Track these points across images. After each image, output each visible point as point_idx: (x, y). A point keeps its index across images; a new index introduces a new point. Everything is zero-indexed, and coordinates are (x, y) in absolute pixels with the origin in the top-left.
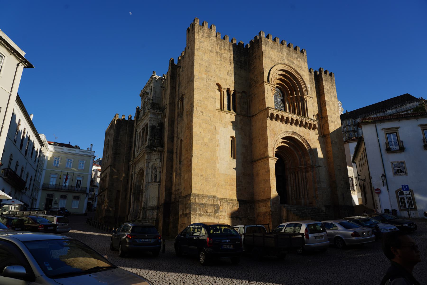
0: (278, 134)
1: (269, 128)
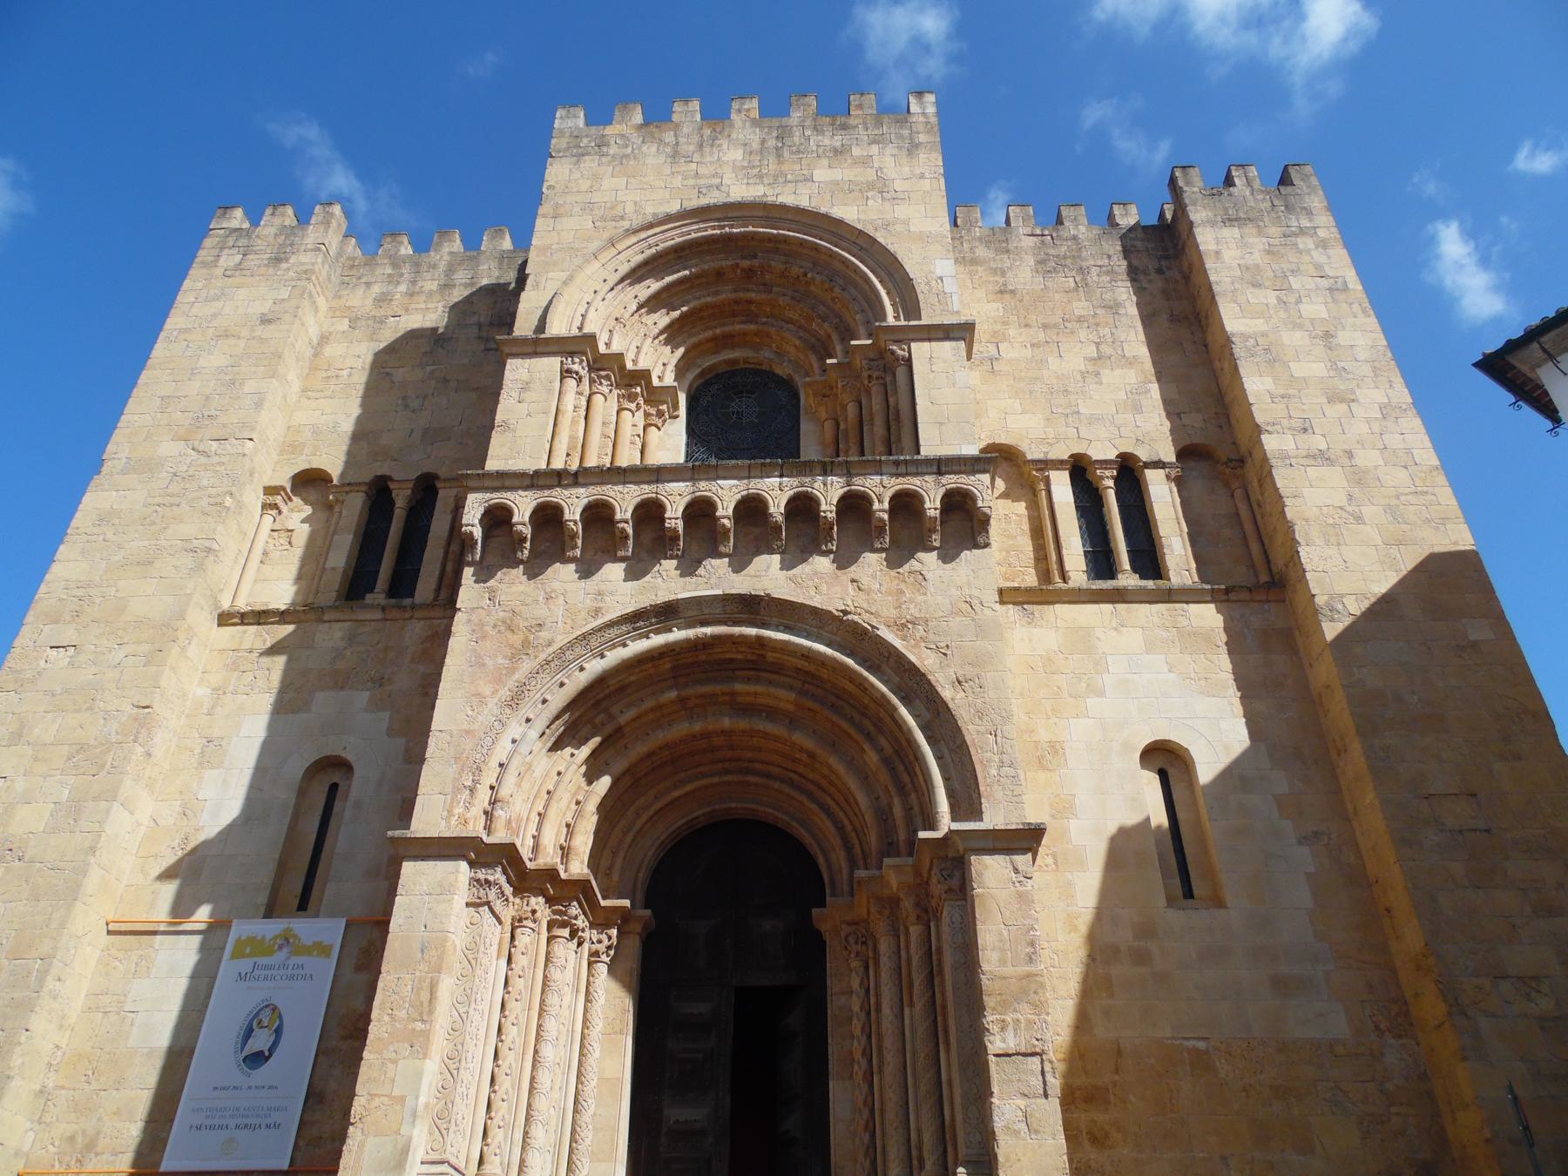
1: (469, 621)
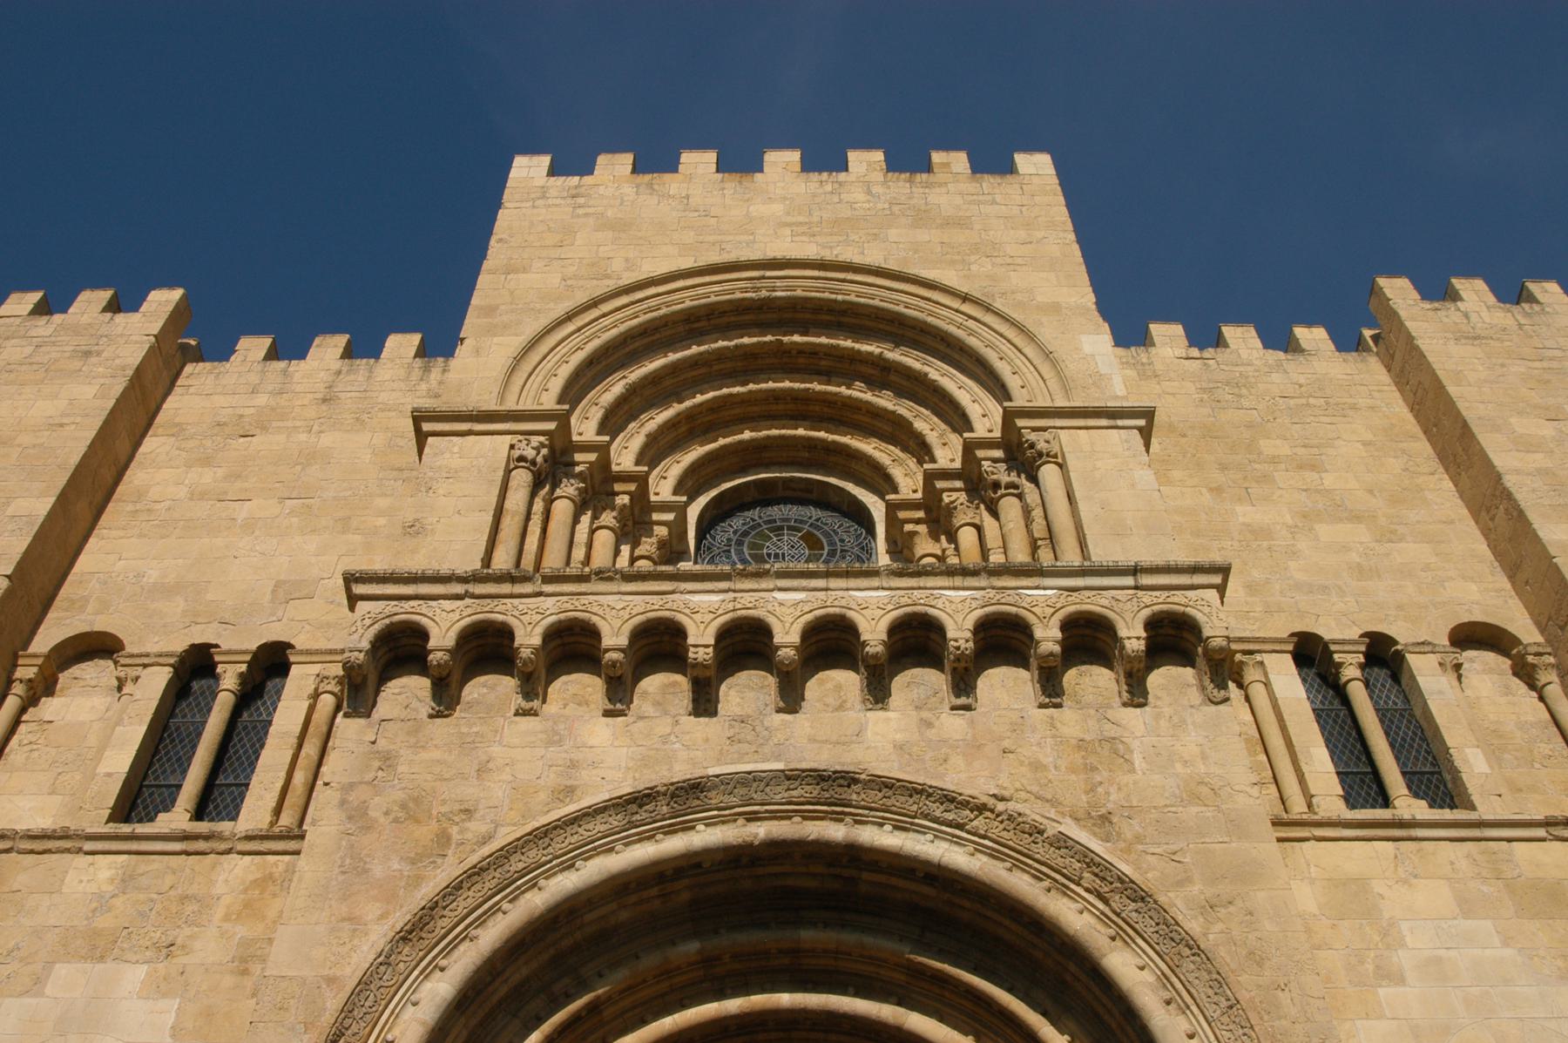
1: (343, 802)
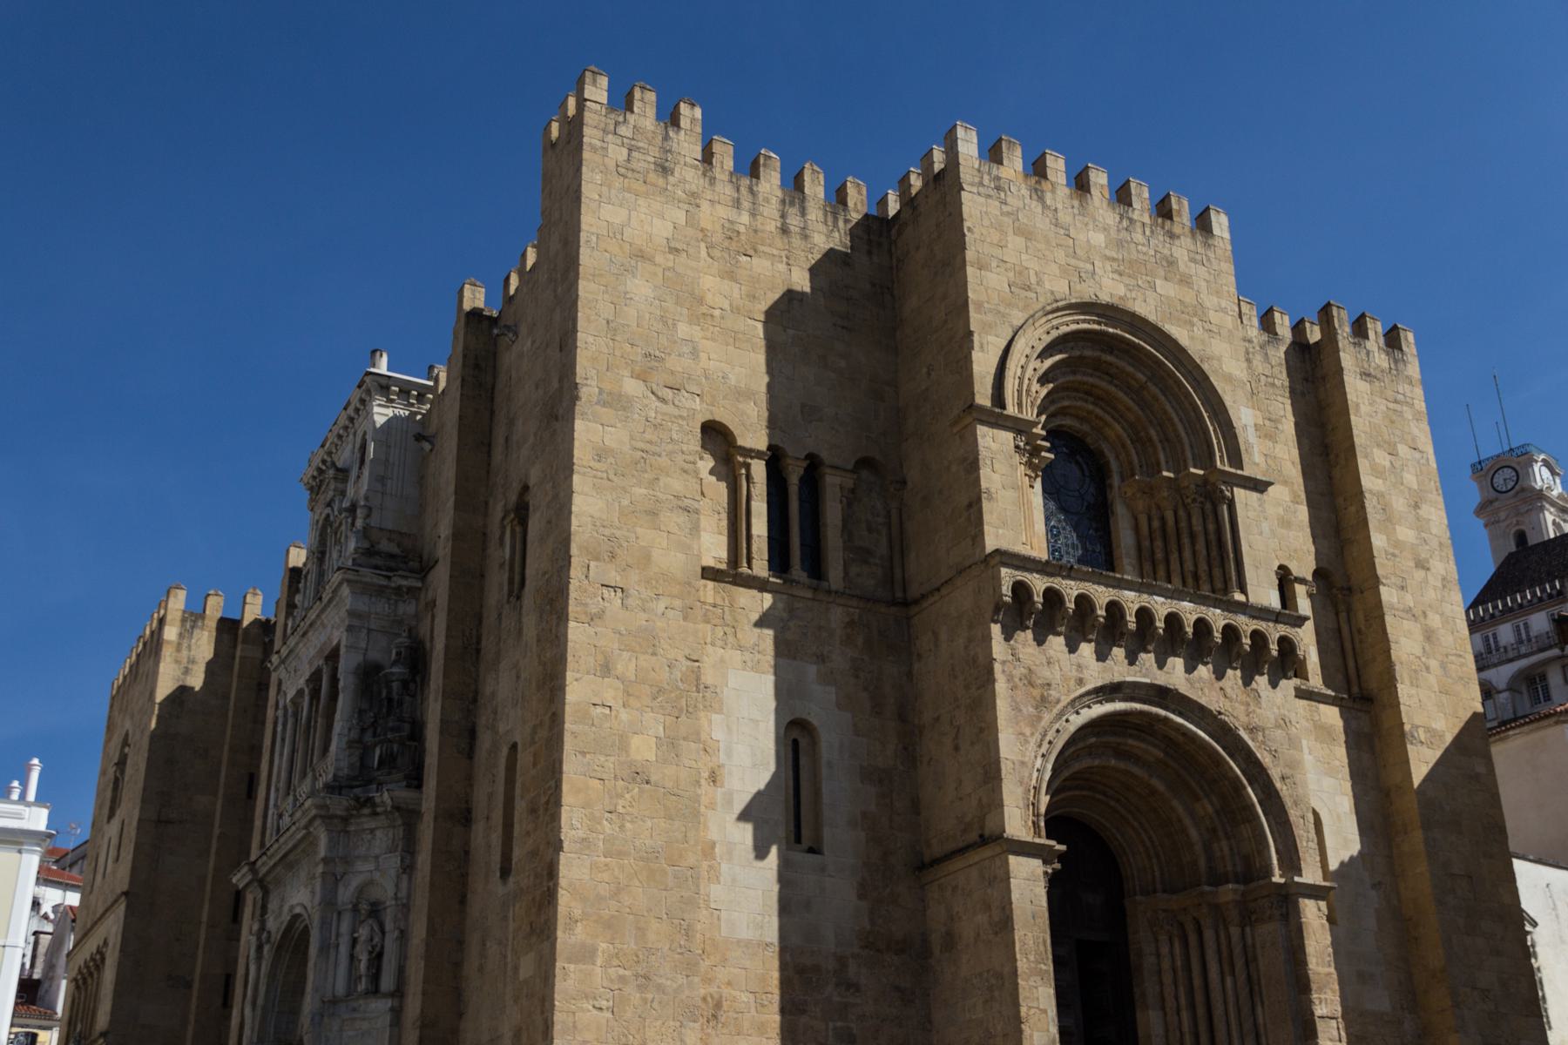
0: (1058, 701)
1: (1004, 671)
